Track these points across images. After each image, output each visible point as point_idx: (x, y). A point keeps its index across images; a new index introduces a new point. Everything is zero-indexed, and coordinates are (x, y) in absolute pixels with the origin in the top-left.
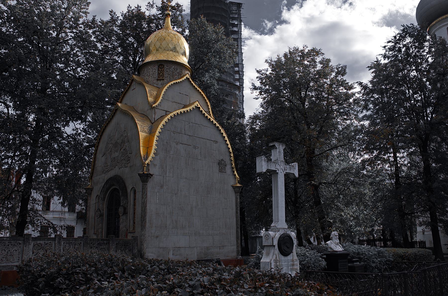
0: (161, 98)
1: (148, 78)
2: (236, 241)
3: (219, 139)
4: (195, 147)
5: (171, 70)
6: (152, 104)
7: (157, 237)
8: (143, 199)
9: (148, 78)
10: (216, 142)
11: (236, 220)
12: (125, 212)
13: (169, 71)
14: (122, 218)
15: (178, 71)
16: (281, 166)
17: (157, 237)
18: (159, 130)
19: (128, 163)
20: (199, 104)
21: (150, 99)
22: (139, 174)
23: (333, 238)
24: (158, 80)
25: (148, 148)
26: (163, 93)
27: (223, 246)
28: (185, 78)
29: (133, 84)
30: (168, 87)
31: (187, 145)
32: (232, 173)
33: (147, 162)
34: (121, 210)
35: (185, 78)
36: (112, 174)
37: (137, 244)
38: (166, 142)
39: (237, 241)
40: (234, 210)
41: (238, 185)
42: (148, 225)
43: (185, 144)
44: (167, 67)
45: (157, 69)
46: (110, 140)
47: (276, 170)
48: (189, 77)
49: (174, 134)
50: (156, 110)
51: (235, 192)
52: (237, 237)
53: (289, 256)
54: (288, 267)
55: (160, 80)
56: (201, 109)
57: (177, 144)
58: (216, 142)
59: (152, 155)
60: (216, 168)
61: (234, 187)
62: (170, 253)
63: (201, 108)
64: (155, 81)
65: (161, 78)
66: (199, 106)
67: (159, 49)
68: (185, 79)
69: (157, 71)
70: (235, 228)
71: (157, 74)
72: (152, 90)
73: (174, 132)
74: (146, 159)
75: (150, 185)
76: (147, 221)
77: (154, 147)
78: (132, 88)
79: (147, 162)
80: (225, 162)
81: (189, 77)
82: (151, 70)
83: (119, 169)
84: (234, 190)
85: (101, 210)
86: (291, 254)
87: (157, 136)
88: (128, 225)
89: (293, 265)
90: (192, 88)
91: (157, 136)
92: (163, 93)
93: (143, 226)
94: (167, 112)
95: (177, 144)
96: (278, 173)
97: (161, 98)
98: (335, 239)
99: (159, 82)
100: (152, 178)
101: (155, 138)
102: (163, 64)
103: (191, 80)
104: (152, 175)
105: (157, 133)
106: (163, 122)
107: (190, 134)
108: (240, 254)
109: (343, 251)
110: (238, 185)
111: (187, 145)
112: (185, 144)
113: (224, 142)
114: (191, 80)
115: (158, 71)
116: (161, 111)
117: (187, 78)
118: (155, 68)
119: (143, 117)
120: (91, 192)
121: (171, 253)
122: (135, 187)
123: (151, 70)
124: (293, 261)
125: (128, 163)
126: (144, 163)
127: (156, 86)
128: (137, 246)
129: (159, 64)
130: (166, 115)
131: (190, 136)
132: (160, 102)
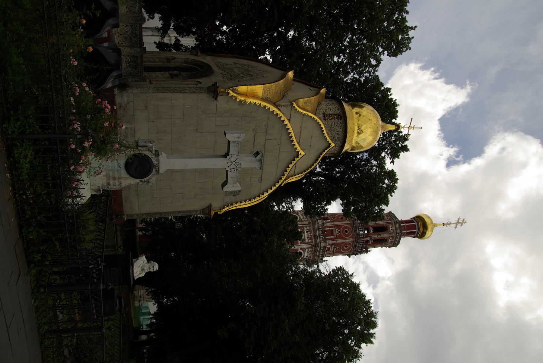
0: (304, 112)
1: (325, 104)
2: (145, 212)
3: (264, 186)
5: (337, 127)
6: (296, 102)
7: (146, 107)
8: (188, 88)
9: (325, 104)
10: (261, 181)
11: (170, 212)
13: (335, 125)
15: (337, 136)
16: (234, 162)
17: (146, 107)
19: (228, 79)
20: (301, 156)
21: (301, 101)
22: (217, 82)
23: (149, 264)
24: (324, 114)
25: (247, 95)
26: (310, 114)
27: (138, 195)
28: (330, 142)
29: (316, 89)
30: (316, 120)
31: (254, 143)
32: (226, 204)
33: (230, 92)
35: (330, 142)
36: (215, 68)
37: (138, 81)
38: (254, 117)
39: (145, 214)
40: (181, 209)
41: (213, 213)
42: (160, 95)
43: (254, 141)
44: (339, 123)
45: (336, 113)
46: (252, 67)
47: (230, 156)
48: (331, 147)
49: (265, 126)
50: (289, 108)
51: (204, 209)
52: (149, 214)
53: (126, 172)
54: (112, 170)
55: (324, 116)
56: (297, 159)
57: (253, 130)
61: (209, 207)
62: (128, 124)
63: (298, 159)
64: (322, 111)
65: (326, 118)
66: (300, 156)
67: (358, 115)
68: (328, 141)
69: (333, 113)
70: (161, 211)
71: (331, 113)
72: (312, 105)
74: (233, 91)
76: (164, 94)
78: (312, 88)
79: (230, 92)
81: (331, 147)
82: (334, 107)
83: (221, 73)
84: (206, 208)
85: (174, 60)
86: (128, 176)
87: (260, 104)
88: (159, 80)
89: (114, 178)
90: (320, 151)
91: (260, 104)
92: (310, 114)
95: (253, 130)
96: (226, 158)
97: (304, 112)
98: (149, 267)
99: (322, 115)
100: (213, 99)
103: (328, 149)
104: (216, 99)
107: (266, 146)
108: (130, 218)
109: (134, 279)
110: (213, 213)
111: (254, 143)
112: (254, 141)
113: (261, 192)
114: (329, 149)
115: (334, 115)
116: (289, 114)
117: (330, 144)
118: (337, 110)
119: (280, 93)
120: (194, 55)
121: (129, 126)
122: (202, 84)
123: (334, 107)
124: (120, 178)
125: (228, 79)
126: (229, 88)
127: (317, 112)
128: (136, 81)
129: (342, 115)
131: (265, 146)
132: (299, 111)
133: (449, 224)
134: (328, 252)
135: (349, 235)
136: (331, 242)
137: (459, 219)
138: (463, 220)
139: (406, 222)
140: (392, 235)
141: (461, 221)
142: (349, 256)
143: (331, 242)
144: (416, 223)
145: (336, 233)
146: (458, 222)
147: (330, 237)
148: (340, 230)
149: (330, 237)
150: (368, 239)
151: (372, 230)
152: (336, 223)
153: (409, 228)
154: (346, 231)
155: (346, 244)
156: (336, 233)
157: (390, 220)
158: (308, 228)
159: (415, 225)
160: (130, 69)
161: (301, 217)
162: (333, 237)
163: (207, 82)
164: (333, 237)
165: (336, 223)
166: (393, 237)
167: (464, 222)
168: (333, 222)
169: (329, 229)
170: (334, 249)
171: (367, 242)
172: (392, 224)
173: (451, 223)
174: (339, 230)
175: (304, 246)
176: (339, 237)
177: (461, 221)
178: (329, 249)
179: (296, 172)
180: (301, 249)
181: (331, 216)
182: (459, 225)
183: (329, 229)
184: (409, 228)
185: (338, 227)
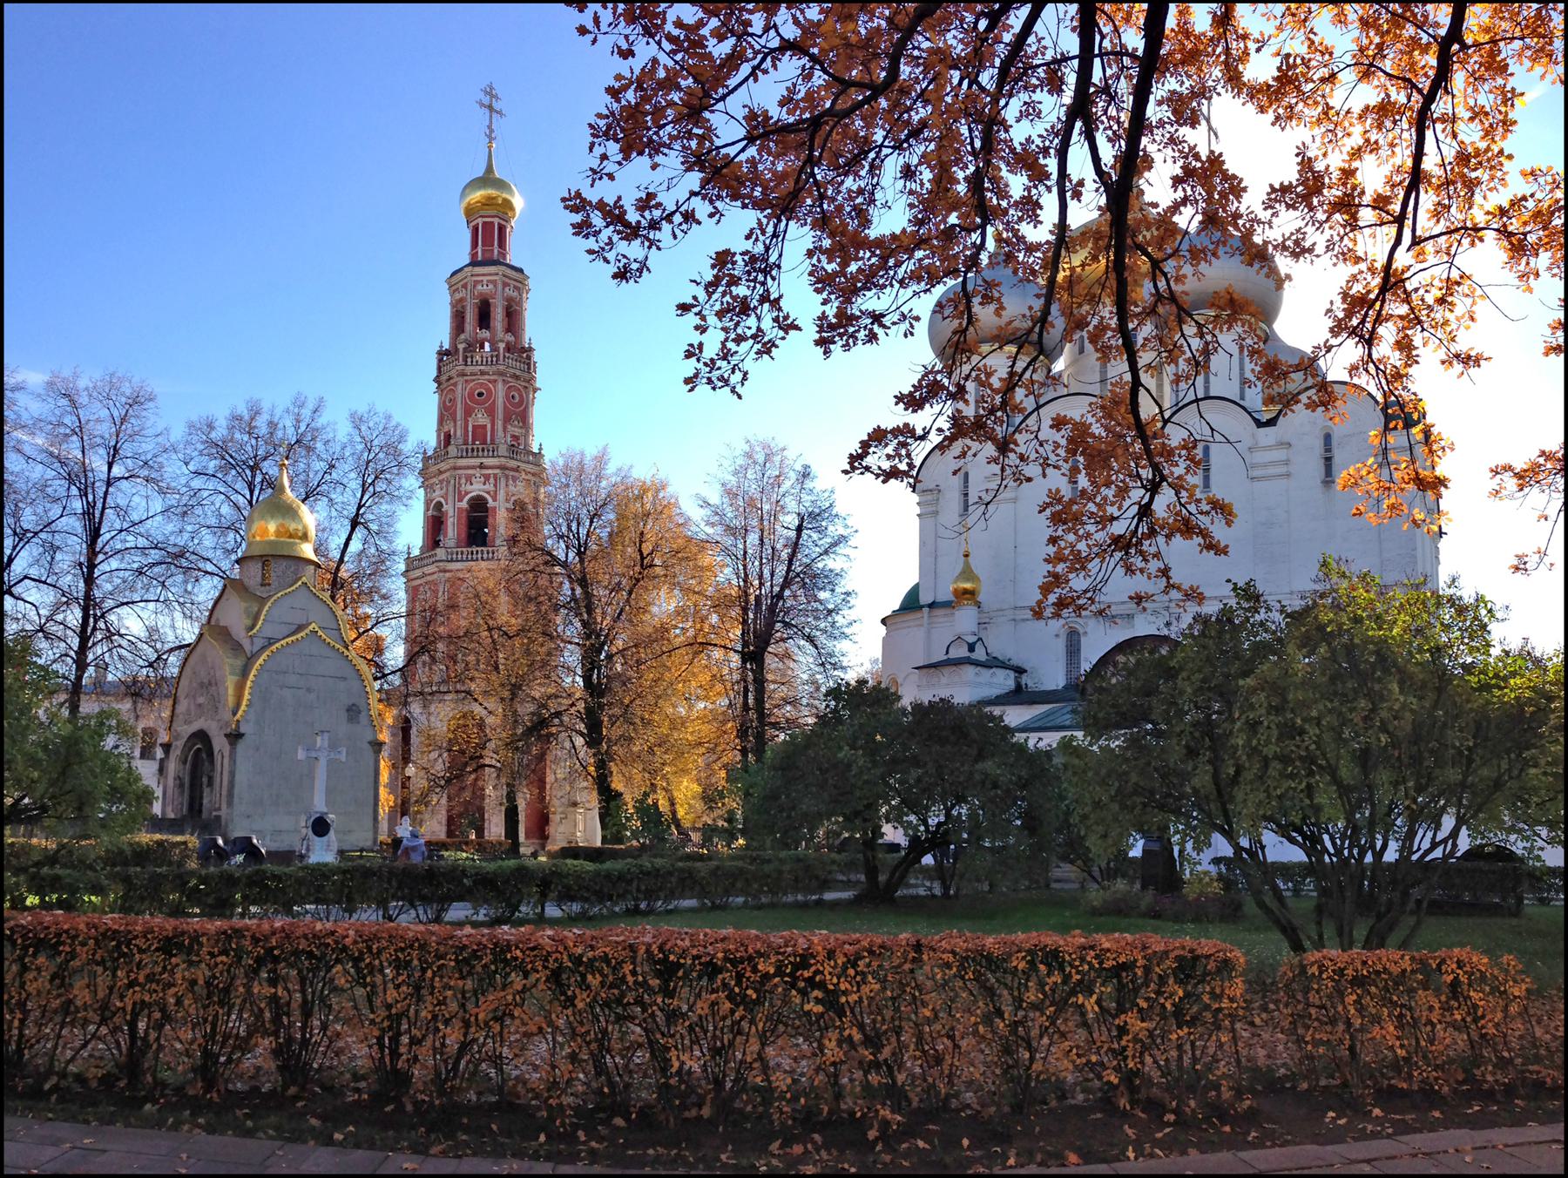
4: (309, 690)
12: (210, 784)
14: (206, 791)
18: (254, 672)
34: (205, 780)
42: (236, 800)
57: (281, 687)
59: (243, 708)
60: (344, 715)
73: (277, 672)
74: (234, 714)
75: (241, 746)
77: (247, 696)
93: (230, 803)
94: (271, 641)
101: (249, 684)
105: (251, 677)
106: (261, 661)
130: (271, 644)
133: (492, 131)
134: (522, 440)
135: (489, 390)
136: (500, 433)
137: (482, 105)
138: (486, 93)
139: (475, 244)
140: (500, 287)
141: (486, 100)
142: (535, 390)
143: (500, 433)
144: (480, 221)
145: (481, 418)
146: (490, 108)
150: (502, 346)
151: (485, 334)
152: (459, 414)
153: (488, 242)
154: (480, 394)
155: (509, 398)
156: (481, 418)
157: (465, 286)
159: (485, 224)
161: (438, 493)
163: (219, 743)
165: (459, 414)
166: (505, 285)
167: (490, 92)
171: (508, 349)
172: (476, 282)
173: (489, 127)
175: (501, 495)
176: (491, 412)
177: (486, 100)
178: (515, 438)
180: (507, 501)
182: (496, 106)
184: (488, 242)
185: (468, 412)
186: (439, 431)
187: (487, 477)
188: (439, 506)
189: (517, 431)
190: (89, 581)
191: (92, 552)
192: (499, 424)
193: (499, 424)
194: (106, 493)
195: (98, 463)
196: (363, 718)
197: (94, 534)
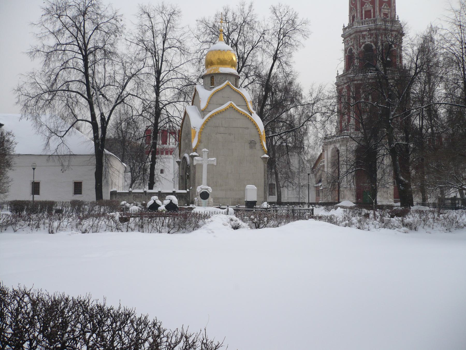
4: (230, 134)
5: (218, 79)
10: (248, 128)
38: (209, 134)
57: (216, 134)
58: (248, 128)
76: (196, 183)
80: (255, 141)
102: (214, 75)
113: (254, 127)
124: (209, 202)
136: (378, 13)
143: (378, 13)
145: (368, 7)
147: (372, 14)
148: (365, 3)
149: (372, 14)
156: (368, 7)
158: (361, 38)
160: (183, 199)
162: (372, 11)
164: (372, 11)
168: (357, 11)
169: (364, 15)
170: (385, 9)
174: (366, 4)
178: (386, 15)
179: (245, 104)
181: (352, 12)
183: (364, 15)
185: (362, 4)
186: (350, 16)
187: (372, 35)
188: (351, 50)
189: (386, 11)
190: (157, 93)
191: (158, 80)
192: (377, 9)
193: (377, 9)
194: (163, 55)
195: (159, 40)
196: (258, 146)
197: (158, 72)
